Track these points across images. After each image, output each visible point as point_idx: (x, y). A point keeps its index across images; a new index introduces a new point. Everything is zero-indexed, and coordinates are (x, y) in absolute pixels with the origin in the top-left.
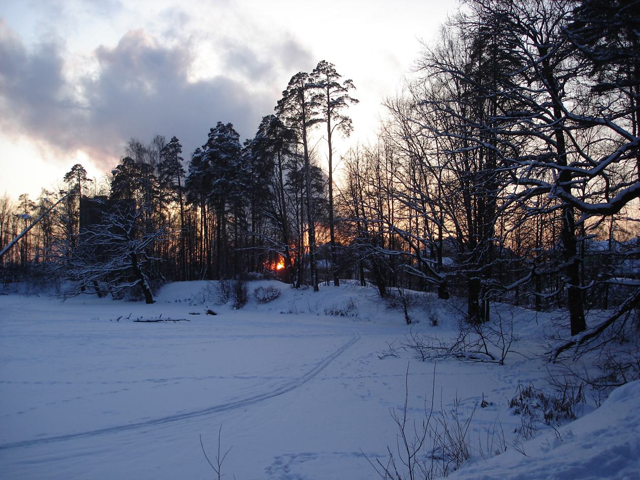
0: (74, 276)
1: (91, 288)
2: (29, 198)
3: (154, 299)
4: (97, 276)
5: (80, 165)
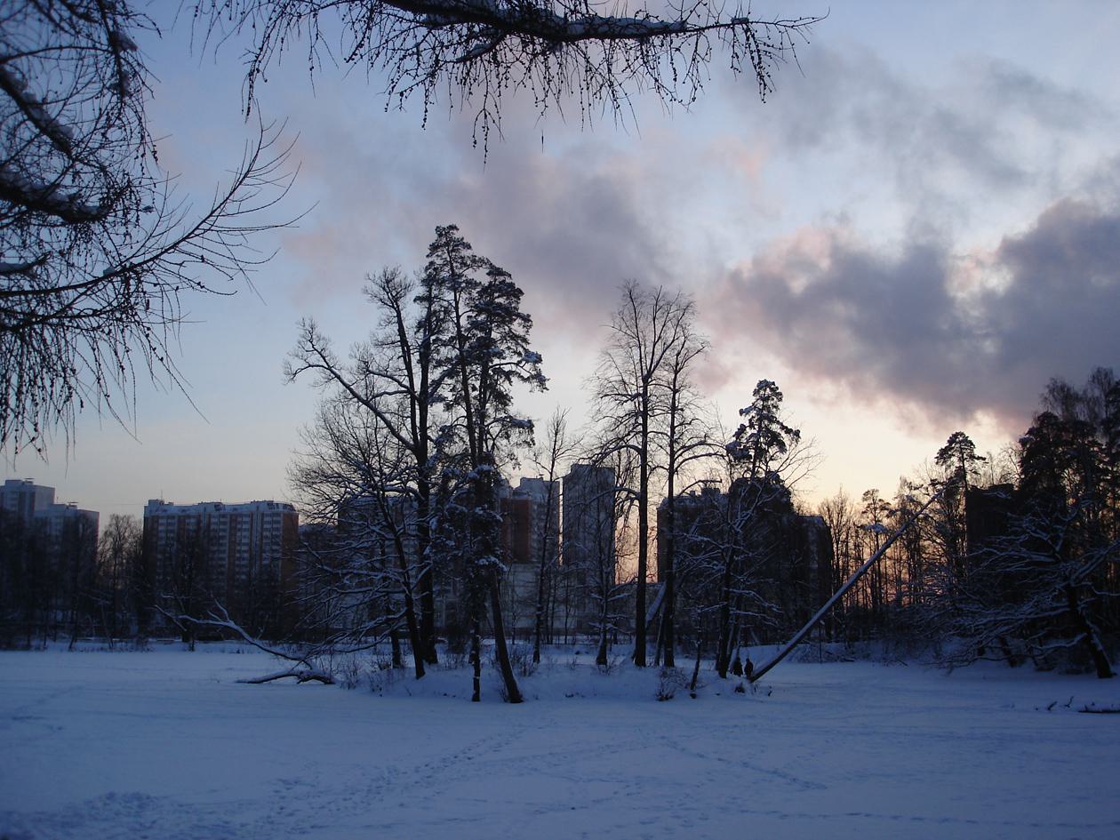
0: (965, 629)
1: (996, 651)
2: (880, 496)
3: (1113, 669)
4: (1006, 628)
5: (962, 434)
